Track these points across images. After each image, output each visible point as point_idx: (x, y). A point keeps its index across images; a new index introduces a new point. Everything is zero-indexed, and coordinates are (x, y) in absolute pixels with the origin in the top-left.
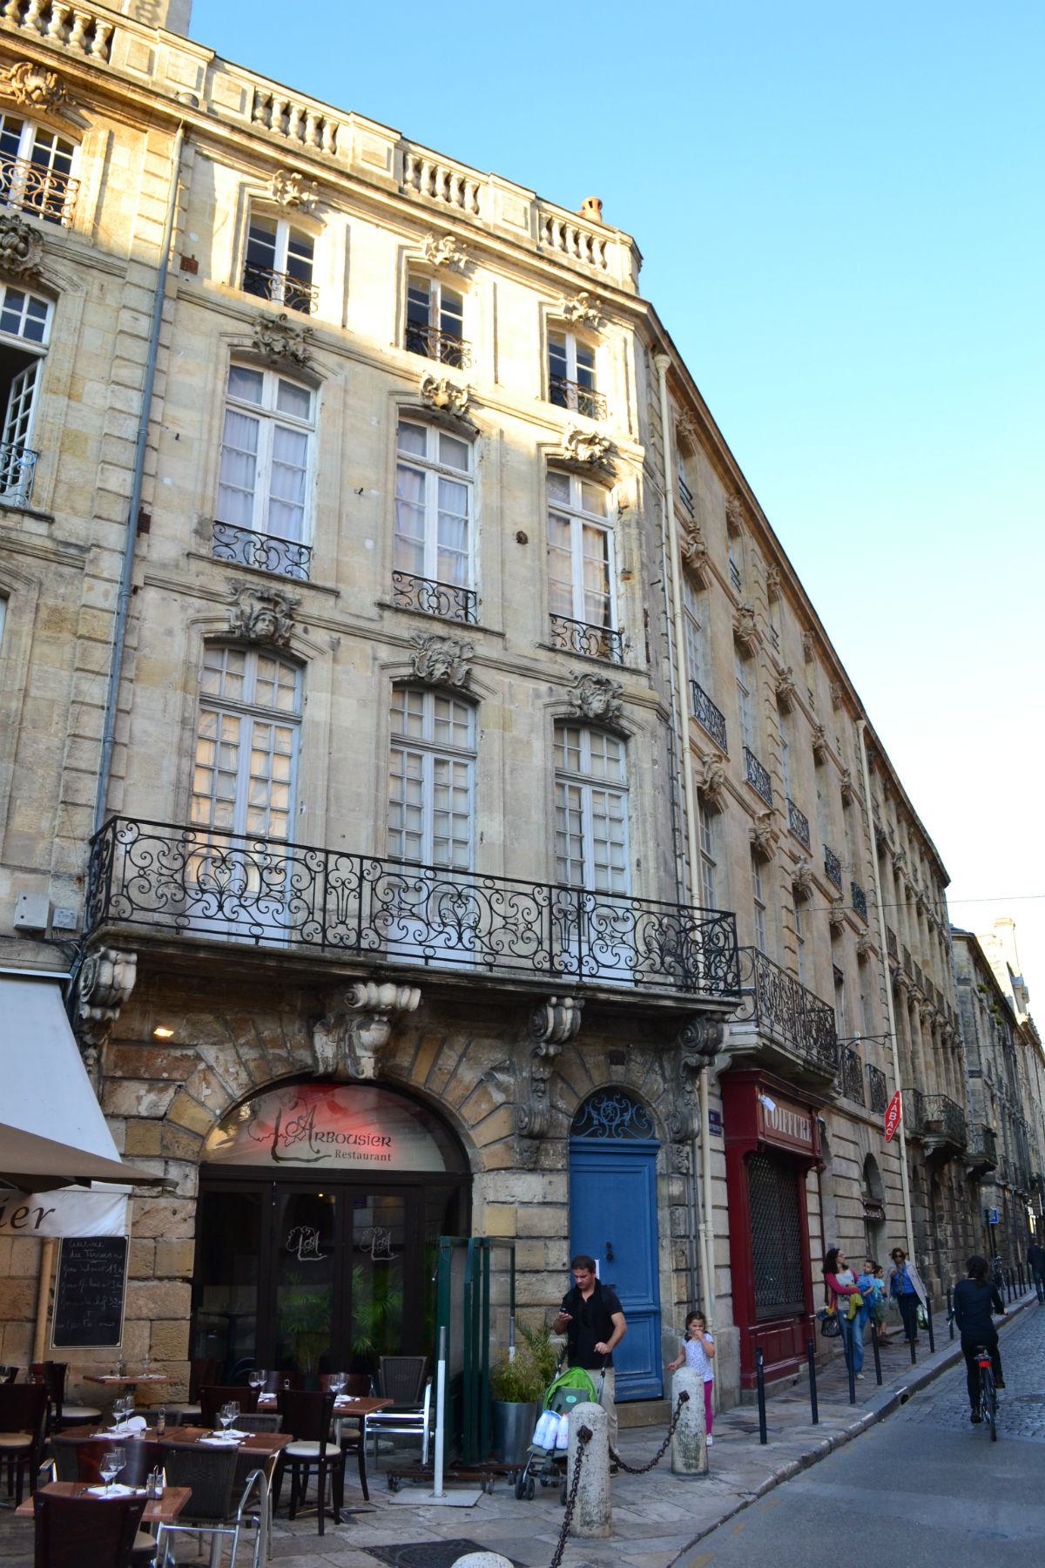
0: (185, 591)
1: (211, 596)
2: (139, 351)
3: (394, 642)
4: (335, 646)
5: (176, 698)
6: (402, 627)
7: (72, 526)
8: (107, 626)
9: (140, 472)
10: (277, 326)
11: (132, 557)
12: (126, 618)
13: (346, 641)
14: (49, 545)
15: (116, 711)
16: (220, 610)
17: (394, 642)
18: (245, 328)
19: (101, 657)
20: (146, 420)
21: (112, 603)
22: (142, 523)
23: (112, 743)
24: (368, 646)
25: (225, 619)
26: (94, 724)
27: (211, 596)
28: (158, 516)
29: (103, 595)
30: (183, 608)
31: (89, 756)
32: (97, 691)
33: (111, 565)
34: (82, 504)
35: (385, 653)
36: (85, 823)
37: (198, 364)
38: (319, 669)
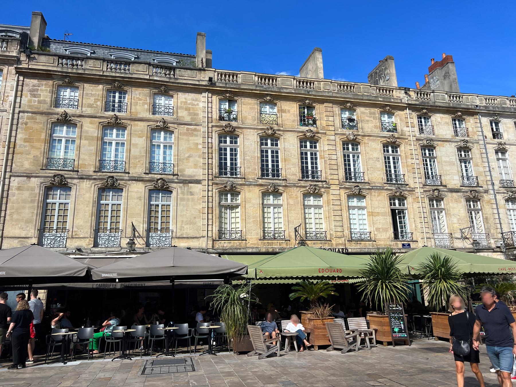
1: (504, 193)
2: (484, 156)
5: (504, 210)
7: (485, 187)
11: (494, 189)
16: (506, 195)
18: (496, 146)
19: (495, 206)
22: (493, 184)
23: (499, 218)
25: (507, 196)
26: (497, 216)
27: (504, 193)
31: (497, 221)
32: (495, 211)
33: (492, 192)
34: (485, 183)
36: (499, 230)
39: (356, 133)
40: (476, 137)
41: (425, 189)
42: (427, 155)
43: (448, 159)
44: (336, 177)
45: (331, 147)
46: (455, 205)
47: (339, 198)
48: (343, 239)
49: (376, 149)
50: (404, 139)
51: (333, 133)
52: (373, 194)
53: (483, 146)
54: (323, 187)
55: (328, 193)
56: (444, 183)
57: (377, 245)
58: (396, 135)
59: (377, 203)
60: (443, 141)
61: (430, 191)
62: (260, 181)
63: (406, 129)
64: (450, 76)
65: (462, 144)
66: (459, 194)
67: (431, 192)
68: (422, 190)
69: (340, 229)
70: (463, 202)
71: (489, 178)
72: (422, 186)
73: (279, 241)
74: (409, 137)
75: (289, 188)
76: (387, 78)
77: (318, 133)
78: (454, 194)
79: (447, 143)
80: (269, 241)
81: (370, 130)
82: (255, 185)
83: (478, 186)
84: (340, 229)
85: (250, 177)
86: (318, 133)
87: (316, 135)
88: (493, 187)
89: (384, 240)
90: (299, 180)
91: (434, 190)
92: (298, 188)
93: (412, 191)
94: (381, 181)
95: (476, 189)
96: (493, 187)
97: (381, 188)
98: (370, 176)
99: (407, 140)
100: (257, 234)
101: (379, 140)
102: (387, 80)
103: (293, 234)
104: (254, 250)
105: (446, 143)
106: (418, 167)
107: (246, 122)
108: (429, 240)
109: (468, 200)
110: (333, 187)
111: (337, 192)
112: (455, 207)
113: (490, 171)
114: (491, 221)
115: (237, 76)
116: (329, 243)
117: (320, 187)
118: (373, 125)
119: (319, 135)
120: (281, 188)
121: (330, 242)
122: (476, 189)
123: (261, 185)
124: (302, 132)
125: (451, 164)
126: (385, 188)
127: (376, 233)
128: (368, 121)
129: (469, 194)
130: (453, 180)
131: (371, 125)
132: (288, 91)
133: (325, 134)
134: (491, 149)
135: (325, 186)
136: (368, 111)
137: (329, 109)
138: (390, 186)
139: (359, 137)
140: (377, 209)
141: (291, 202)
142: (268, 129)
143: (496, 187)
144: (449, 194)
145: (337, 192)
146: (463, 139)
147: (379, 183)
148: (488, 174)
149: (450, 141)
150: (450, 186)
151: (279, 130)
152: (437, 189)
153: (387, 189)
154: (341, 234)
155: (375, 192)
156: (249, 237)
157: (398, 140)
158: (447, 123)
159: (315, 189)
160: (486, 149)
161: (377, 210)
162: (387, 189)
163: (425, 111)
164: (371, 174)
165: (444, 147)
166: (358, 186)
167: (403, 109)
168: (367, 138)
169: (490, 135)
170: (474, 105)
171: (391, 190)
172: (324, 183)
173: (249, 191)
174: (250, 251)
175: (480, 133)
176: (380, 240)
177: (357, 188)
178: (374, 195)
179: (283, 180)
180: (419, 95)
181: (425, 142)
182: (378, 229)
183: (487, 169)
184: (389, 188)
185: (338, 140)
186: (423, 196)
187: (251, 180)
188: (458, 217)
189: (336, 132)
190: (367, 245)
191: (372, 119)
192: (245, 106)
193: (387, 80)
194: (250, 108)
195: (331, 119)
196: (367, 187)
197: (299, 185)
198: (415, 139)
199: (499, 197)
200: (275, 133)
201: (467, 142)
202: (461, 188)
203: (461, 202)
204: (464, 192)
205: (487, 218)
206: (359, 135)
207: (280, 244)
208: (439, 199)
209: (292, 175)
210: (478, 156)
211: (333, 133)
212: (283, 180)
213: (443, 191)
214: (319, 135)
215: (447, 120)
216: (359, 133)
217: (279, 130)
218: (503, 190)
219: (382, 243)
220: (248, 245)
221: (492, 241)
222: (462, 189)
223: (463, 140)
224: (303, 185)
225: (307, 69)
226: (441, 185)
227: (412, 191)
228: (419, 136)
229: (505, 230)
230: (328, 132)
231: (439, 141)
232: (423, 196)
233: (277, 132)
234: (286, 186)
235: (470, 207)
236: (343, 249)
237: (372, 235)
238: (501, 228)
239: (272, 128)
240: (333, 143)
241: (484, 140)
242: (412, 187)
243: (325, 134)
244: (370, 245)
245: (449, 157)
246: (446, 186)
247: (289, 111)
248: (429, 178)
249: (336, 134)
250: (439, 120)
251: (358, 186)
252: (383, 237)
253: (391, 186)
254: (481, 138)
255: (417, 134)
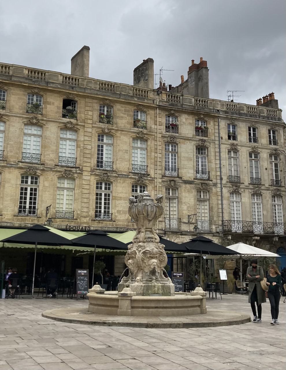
0: (227, 187)
2: (218, 154)
3: (251, 189)
4: (244, 191)
6: (251, 187)
7: (214, 181)
8: (219, 194)
9: (221, 172)
10: (233, 145)
11: (221, 184)
12: (221, 192)
13: (245, 190)
14: (213, 184)
15: (222, 204)
16: (231, 189)
17: (251, 189)
19: (220, 198)
20: (220, 164)
21: (220, 191)
22: (221, 179)
23: (222, 208)
24: (248, 190)
26: (220, 206)
28: (223, 177)
29: (219, 190)
30: (227, 189)
31: (220, 211)
32: (220, 202)
33: (219, 185)
34: (215, 177)
35: (250, 190)
36: (221, 218)
37: (224, 155)
38: (242, 194)
39: (111, 127)
40: (213, 138)
41: (163, 180)
42: (170, 150)
43: (186, 155)
44: (88, 164)
45: (86, 138)
46: (187, 195)
47: (89, 183)
48: (88, 218)
49: (126, 142)
50: (152, 135)
51: (90, 126)
52: (119, 181)
53: (217, 146)
54: (76, 173)
55: (81, 178)
56: (180, 175)
57: (116, 225)
58: (145, 131)
59: (121, 189)
60: (185, 139)
61: (167, 181)
62: (21, 164)
63: (153, 126)
64: (202, 79)
65: (200, 143)
66: (192, 185)
67: (168, 182)
68: (160, 180)
69: (85, 210)
70: (194, 193)
71: (219, 173)
72: (161, 177)
73: (31, 218)
74: (156, 134)
75: (46, 172)
76: (147, 78)
77: (77, 125)
78: (188, 186)
79: (188, 142)
80: (23, 217)
81: (123, 125)
82: (15, 168)
83: (209, 179)
84: (85, 210)
85: (12, 160)
86: (77, 125)
87: (76, 126)
88: (221, 182)
89: (123, 221)
90: (55, 165)
91: (170, 181)
92: (54, 173)
93: (152, 180)
94: (127, 170)
95: (207, 182)
96: (221, 182)
97: (127, 176)
98: (118, 166)
99: (154, 137)
100: (13, 210)
101: (130, 134)
102: (146, 80)
103: (44, 212)
104: (9, 225)
105: (187, 141)
106: (160, 160)
107: (13, 110)
108: (161, 223)
109: (199, 191)
110: (85, 173)
111: (88, 178)
112: (188, 196)
113: (220, 168)
114: (215, 210)
115: (9, 68)
116: (75, 222)
117: (73, 173)
118: (126, 121)
119: (78, 127)
120: (38, 171)
121: (76, 221)
122: (207, 182)
123: (21, 168)
124: (63, 123)
125: (189, 159)
126: (130, 176)
127: (116, 214)
128: (122, 117)
129: (200, 186)
130: (189, 173)
131: (124, 121)
132: (54, 85)
133: (84, 126)
134: (224, 148)
135: (78, 172)
136: (123, 109)
137: (89, 104)
138: (134, 175)
139: (113, 131)
140: (121, 195)
141: (47, 184)
142: (32, 118)
143: (224, 182)
144: (184, 186)
145: (88, 178)
146: (202, 138)
147: (126, 172)
148: (218, 170)
149: (191, 140)
150: (185, 178)
151: (43, 120)
152: (173, 180)
153: (131, 178)
154: (86, 214)
155: (120, 180)
156: (5, 213)
157: (146, 136)
158: (190, 124)
159: (69, 174)
160: (220, 148)
161: (120, 195)
162: (131, 178)
163: (172, 112)
164: (119, 164)
165: (185, 144)
166: (107, 174)
167: (154, 108)
168: (119, 132)
169: (225, 136)
170: (216, 109)
171: (135, 179)
172: (78, 169)
173: (10, 173)
174: (5, 224)
175: (217, 135)
176: (119, 221)
177: (105, 175)
178: (120, 182)
179: (42, 164)
180: (170, 97)
181: (169, 139)
182: (119, 212)
183: (218, 166)
184: (133, 177)
185: (94, 132)
186: (161, 185)
187: (12, 163)
188: (188, 205)
189: (94, 125)
190: (108, 224)
191: (126, 116)
192: (13, 96)
193: (146, 80)
194: (18, 98)
195: (90, 113)
196: (115, 175)
197: (56, 169)
198: (160, 135)
199: (225, 190)
200: (39, 122)
201: (205, 141)
202: (195, 180)
203: (192, 192)
204: (196, 184)
205: (212, 208)
206: (113, 129)
207: (32, 220)
208: (175, 189)
209: (50, 161)
210: (213, 154)
211: (90, 126)
212: (42, 164)
213: (179, 182)
214: (78, 127)
215: (191, 121)
216: (114, 128)
217: (43, 120)
218: (229, 185)
219: (121, 223)
220: (4, 220)
221: (214, 227)
222: (195, 181)
223: (201, 140)
224: (59, 170)
225: (77, 61)
226: (178, 177)
227: (152, 180)
228: (165, 133)
229: (226, 218)
230: (86, 125)
231: (181, 139)
232: (161, 185)
233: (41, 121)
234: (43, 170)
235: (200, 197)
236: (85, 227)
237: (113, 216)
238: (223, 217)
239: (36, 118)
240: (90, 134)
241: (219, 141)
242: (153, 176)
243: (84, 126)
244: (110, 224)
245: (188, 153)
246: (181, 178)
247: (53, 104)
248: (169, 170)
249: (93, 127)
250: (184, 120)
251: (107, 174)
252: (122, 218)
253: (135, 175)
254: (217, 139)
255: (164, 131)
